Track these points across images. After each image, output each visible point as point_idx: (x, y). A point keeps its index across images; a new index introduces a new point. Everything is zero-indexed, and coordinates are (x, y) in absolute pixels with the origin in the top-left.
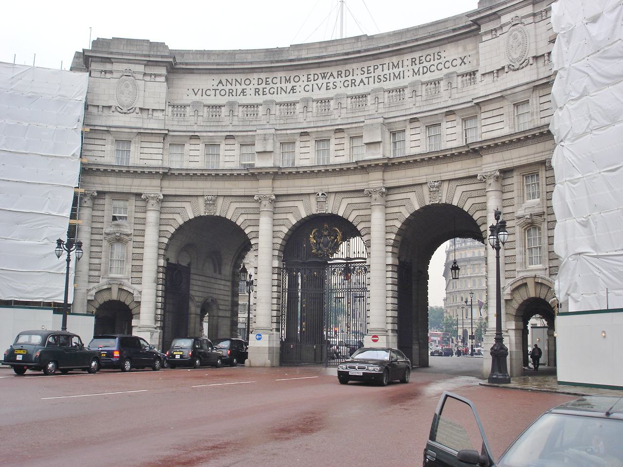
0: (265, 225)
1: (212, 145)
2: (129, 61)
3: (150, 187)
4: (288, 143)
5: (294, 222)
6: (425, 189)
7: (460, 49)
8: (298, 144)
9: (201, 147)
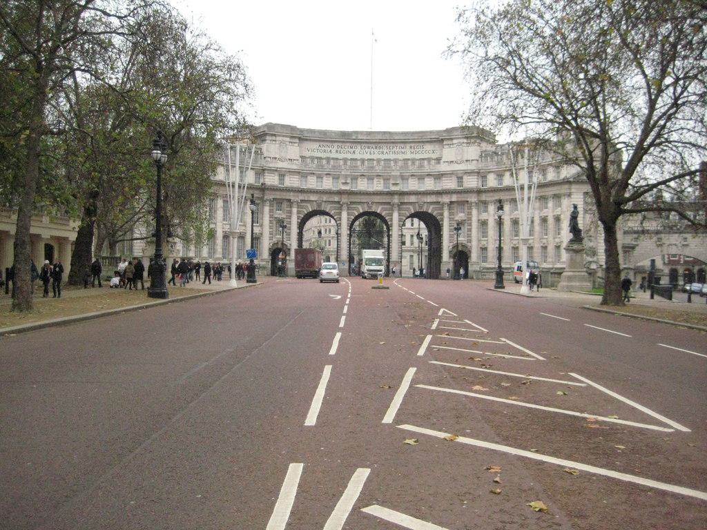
0: (344, 215)
1: (320, 177)
2: (283, 136)
3: (292, 196)
4: (355, 178)
5: (357, 214)
6: (417, 205)
7: (432, 146)
8: (359, 180)
9: (315, 178)
